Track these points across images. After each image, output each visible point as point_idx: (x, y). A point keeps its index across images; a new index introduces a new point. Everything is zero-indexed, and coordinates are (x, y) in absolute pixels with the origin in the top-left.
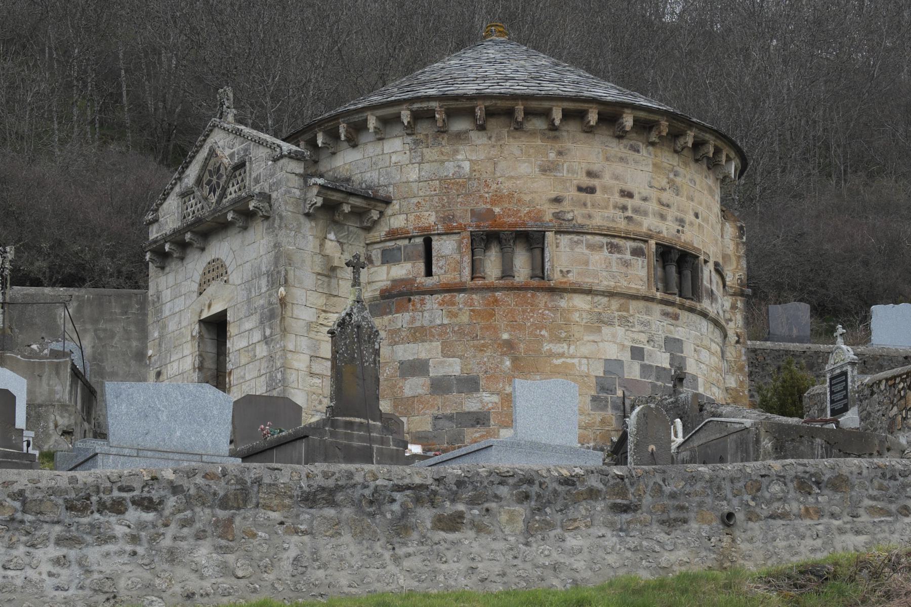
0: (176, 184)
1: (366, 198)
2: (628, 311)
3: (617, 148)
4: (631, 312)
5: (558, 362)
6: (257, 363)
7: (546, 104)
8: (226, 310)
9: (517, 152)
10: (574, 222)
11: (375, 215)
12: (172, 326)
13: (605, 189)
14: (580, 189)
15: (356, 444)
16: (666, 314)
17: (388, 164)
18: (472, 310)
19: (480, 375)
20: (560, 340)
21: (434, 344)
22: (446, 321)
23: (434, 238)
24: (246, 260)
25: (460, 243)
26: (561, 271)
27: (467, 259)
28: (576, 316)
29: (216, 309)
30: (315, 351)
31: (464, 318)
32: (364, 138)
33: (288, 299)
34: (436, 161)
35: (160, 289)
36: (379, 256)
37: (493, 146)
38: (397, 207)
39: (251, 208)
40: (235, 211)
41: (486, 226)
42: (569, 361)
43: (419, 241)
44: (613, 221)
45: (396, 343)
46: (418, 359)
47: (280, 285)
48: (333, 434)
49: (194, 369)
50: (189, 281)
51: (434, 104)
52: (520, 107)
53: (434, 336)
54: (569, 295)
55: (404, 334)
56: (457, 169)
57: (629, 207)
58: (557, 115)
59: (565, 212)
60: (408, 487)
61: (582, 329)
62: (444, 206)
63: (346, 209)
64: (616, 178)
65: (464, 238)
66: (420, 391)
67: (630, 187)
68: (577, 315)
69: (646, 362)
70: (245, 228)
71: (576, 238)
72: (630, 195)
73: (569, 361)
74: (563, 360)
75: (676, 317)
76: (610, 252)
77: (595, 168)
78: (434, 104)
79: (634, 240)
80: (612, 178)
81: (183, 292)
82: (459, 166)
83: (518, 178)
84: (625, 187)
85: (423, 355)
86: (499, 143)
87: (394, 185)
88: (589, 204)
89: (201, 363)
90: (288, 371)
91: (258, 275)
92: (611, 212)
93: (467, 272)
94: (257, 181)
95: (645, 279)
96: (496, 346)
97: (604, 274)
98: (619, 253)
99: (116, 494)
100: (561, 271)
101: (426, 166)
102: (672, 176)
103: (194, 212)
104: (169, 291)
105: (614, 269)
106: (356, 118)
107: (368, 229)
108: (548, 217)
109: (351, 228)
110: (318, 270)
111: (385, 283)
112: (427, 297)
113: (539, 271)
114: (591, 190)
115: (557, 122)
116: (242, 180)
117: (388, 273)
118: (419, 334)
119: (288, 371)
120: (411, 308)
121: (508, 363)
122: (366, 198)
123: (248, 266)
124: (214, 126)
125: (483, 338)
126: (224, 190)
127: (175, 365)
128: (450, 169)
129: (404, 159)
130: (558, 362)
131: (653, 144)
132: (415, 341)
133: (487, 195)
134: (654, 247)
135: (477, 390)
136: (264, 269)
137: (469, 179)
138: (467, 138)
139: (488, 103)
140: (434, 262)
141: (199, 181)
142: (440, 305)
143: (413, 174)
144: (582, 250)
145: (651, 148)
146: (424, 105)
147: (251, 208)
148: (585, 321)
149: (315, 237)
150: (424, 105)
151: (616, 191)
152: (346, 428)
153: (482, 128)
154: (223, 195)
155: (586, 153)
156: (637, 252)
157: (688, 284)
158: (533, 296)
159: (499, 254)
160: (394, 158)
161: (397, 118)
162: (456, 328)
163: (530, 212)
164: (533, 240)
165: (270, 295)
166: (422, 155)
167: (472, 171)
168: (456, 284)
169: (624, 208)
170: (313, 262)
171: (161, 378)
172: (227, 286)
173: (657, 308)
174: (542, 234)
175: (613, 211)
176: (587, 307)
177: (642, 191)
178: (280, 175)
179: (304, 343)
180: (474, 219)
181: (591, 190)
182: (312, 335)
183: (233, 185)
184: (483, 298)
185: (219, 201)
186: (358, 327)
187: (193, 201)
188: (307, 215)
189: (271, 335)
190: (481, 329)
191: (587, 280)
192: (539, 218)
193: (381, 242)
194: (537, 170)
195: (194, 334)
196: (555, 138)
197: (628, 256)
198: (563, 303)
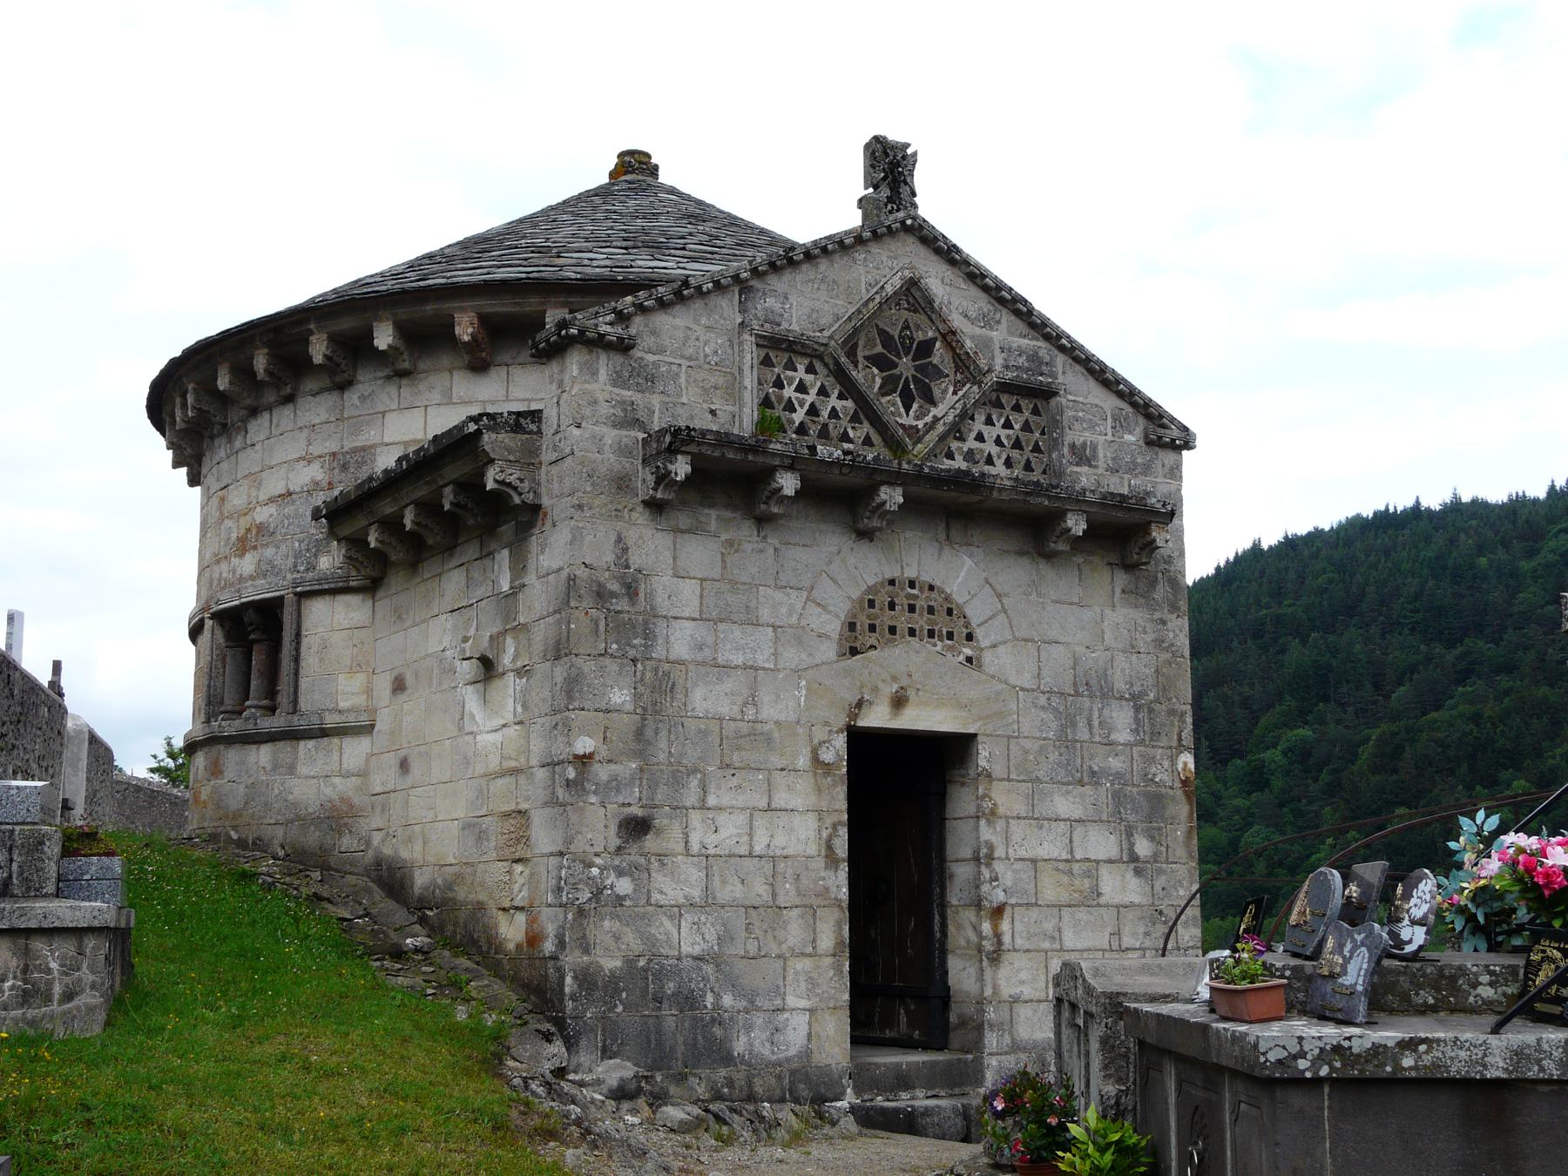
8: (972, 738)
12: (708, 699)
24: (1053, 634)
29: (922, 718)
123: (1057, 657)
171: (650, 842)
189: (1155, 857)
195: (827, 756)
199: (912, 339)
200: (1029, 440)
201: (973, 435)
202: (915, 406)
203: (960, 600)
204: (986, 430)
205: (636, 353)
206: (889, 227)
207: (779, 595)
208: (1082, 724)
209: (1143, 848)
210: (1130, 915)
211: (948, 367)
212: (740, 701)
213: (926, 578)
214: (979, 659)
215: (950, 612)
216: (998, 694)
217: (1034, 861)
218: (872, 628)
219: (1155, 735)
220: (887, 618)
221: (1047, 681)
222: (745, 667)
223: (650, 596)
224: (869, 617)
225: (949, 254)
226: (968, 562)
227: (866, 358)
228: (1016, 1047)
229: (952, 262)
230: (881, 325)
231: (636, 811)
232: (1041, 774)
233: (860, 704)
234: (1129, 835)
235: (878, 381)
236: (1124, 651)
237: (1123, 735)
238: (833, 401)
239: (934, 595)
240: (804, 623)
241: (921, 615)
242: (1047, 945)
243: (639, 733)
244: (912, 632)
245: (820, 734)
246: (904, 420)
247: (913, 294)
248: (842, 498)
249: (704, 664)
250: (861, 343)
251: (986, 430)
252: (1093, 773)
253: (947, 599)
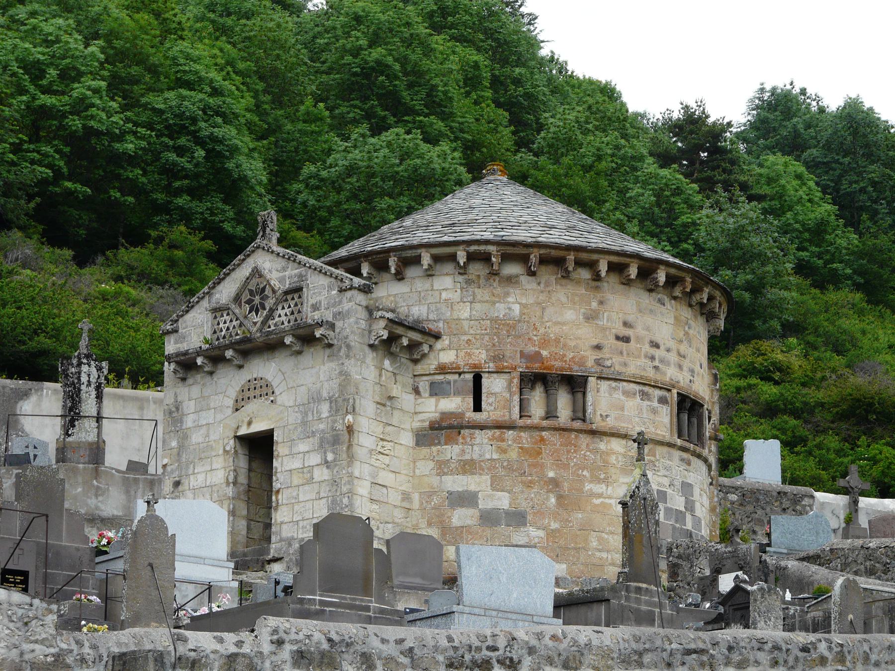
0: (203, 298)
1: (423, 332)
2: (655, 456)
3: (646, 300)
4: (658, 457)
5: (597, 501)
6: (316, 486)
7: (595, 257)
8: (272, 431)
9: (564, 300)
10: (612, 369)
11: (425, 348)
12: (196, 438)
13: (639, 339)
14: (618, 338)
15: (644, 608)
16: (682, 460)
17: (438, 300)
18: (521, 448)
19: (528, 510)
20: (599, 481)
21: (484, 477)
22: (495, 456)
23: (485, 376)
24: (301, 383)
25: (510, 382)
26: (601, 415)
27: (516, 398)
28: (613, 459)
29: (258, 427)
30: (374, 478)
31: (513, 455)
32: (411, 272)
33: (355, 427)
34: (487, 301)
35: (179, 399)
36: (427, 388)
37: (542, 292)
38: (447, 342)
39: (318, 336)
40: (293, 335)
41: (536, 368)
42: (607, 501)
43: (470, 377)
44: (645, 370)
45: (445, 474)
46: (467, 491)
47: (347, 413)
48: (627, 598)
49: (228, 484)
50: (221, 396)
51: (492, 249)
52: (571, 257)
53: (483, 470)
54: (608, 438)
55: (453, 466)
56: (507, 311)
57: (657, 357)
58: (603, 267)
59: (604, 359)
60: (695, 651)
61: (618, 472)
62: (494, 345)
63: (405, 342)
64: (648, 329)
65: (514, 378)
66: (469, 522)
67: (658, 339)
68: (614, 457)
69: (669, 505)
70: (299, 353)
71: (614, 384)
72: (657, 346)
73: (607, 501)
74: (601, 500)
75: (689, 463)
76: (642, 399)
77: (630, 319)
78: (492, 249)
79: (661, 388)
80: (643, 329)
81: (212, 405)
82: (510, 309)
83: (564, 324)
84: (653, 339)
85: (473, 488)
86: (548, 289)
87: (444, 321)
88: (625, 353)
89: (236, 477)
90: (355, 497)
91: (316, 398)
92: (642, 362)
93: (516, 410)
94: (315, 307)
95: (668, 426)
96: (542, 483)
97: (637, 419)
98: (649, 400)
99: (486, 653)
100: (601, 415)
101: (477, 306)
102: (687, 329)
103: (228, 329)
104: (192, 403)
105: (645, 416)
106: (409, 253)
107: (416, 362)
108: (590, 363)
109: (403, 360)
110: (378, 399)
111: (431, 415)
112: (477, 431)
113: (580, 413)
114: (626, 340)
115: (603, 274)
116: (296, 305)
117: (436, 406)
118: (468, 467)
119: (355, 497)
120: (461, 440)
121: (553, 500)
122: (423, 332)
123: (303, 389)
124: (258, 247)
125: (531, 475)
126: (272, 311)
127: (201, 478)
128: (500, 310)
129: (456, 296)
130: (597, 501)
131: (675, 298)
132: (464, 472)
133: (535, 338)
134: (676, 395)
135: (525, 524)
136: (325, 394)
137: (519, 321)
138: (517, 282)
139: (542, 251)
140: (483, 398)
141: (237, 299)
142: (490, 440)
143: (464, 312)
144: (619, 395)
145: (673, 302)
146: (482, 248)
147: (318, 336)
148: (620, 463)
149: (376, 367)
150: (482, 248)
151: (647, 340)
152: (636, 593)
153: (532, 274)
154: (270, 316)
155: (625, 305)
156: (663, 401)
157: (694, 431)
158: (576, 437)
159: (543, 395)
160: (444, 295)
161: (453, 258)
162: (505, 464)
163: (573, 358)
164: (576, 384)
165: (335, 421)
166: (474, 292)
167: (522, 314)
168: (505, 421)
169: (653, 358)
170: (374, 391)
171: (180, 488)
172: (274, 406)
173: (677, 454)
174: (585, 379)
175: (644, 360)
176: (622, 450)
177: (666, 342)
178: (346, 306)
179: (366, 469)
180: (523, 360)
181: (626, 340)
182: (373, 462)
183: (283, 308)
184: (531, 437)
185: (264, 322)
186: (645, 499)
187: (225, 317)
188: (371, 346)
189: (335, 460)
190: (529, 465)
191: (623, 425)
192: (582, 363)
193: (430, 374)
194: (581, 317)
195: (228, 448)
196: (597, 288)
197: (655, 404)
198: (602, 446)
200: (296, 310)
205: (180, 331)
209: (330, 457)
210: (324, 484)
213: (260, 376)
217: (290, 471)
219: (337, 411)
221: (299, 401)
226: (274, 365)
228: (281, 540)
231: (177, 479)
232: (294, 437)
233: (238, 428)
234: (325, 453)
237: (325, 414)
242: (293, 501)
243: (178, 454)
244: (255, 397)
245: (226, 441)
252: (313, 432)
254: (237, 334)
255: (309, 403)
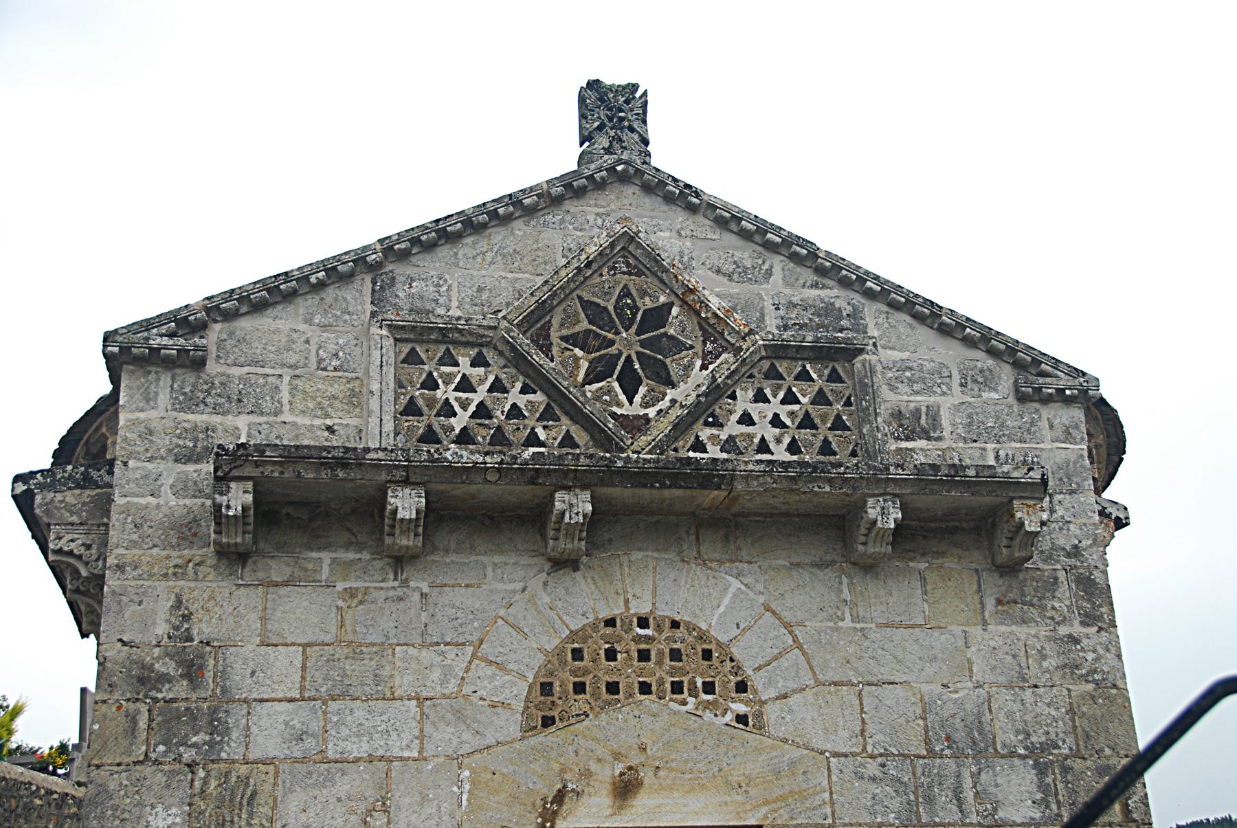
24: (884, 673)
199: (634, 308)
200: (824, 416)
201: (735, 417)
202: (642, 390)
203: (724, 638)
204: (755, 410)
206: (590, 178)
207: (427, 655)
208: (943, 797)
211: (693, 338)
212: (362, 808)
213: (666, 612)
214: (759, 715)
215: (707, 655)
216: (793, 764)
218: (580, 688)
220: (605, 671)
221: (878, 739)
222: (371, 759)
223: (222, 674)
224: (574, 673)
225: (685, 198)
226: (735, 584)
227: (563, 338)
229: (692, 209)
230: (586, 296)
233: (560, 797)
235: (584, 365)
236: (1009, 687)
238: (515, 396)
239: (678, 634)
240: (467, 689)
241: (660, 663)
244: (645, 688)
246: (625, 410)
247: (627, 251)
248: (490, 512)
249: (304, 760)
250: (556, 322)
251: (755, 410)
253: (702, 637)
254: (533, 440)
255: (931, 753)
